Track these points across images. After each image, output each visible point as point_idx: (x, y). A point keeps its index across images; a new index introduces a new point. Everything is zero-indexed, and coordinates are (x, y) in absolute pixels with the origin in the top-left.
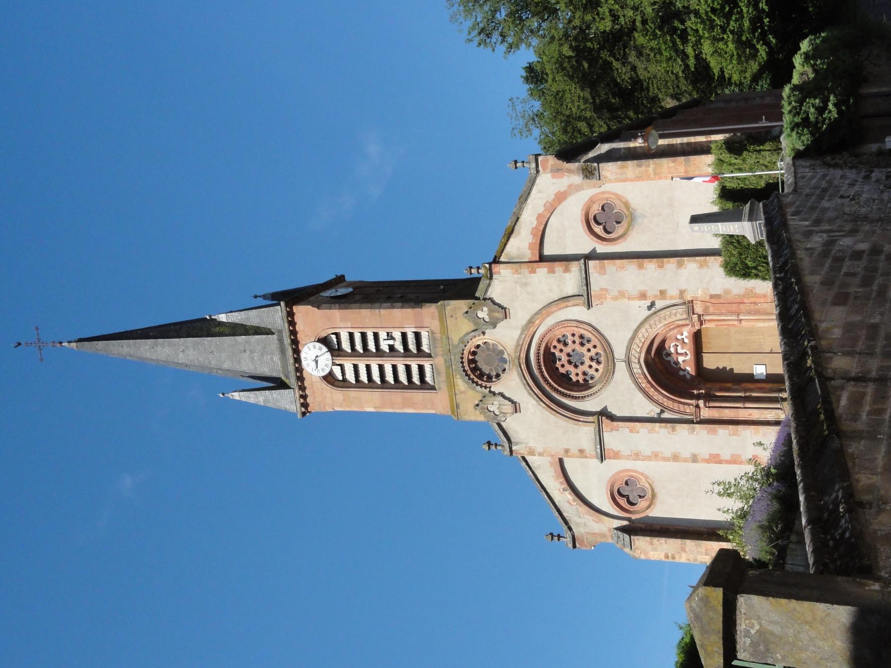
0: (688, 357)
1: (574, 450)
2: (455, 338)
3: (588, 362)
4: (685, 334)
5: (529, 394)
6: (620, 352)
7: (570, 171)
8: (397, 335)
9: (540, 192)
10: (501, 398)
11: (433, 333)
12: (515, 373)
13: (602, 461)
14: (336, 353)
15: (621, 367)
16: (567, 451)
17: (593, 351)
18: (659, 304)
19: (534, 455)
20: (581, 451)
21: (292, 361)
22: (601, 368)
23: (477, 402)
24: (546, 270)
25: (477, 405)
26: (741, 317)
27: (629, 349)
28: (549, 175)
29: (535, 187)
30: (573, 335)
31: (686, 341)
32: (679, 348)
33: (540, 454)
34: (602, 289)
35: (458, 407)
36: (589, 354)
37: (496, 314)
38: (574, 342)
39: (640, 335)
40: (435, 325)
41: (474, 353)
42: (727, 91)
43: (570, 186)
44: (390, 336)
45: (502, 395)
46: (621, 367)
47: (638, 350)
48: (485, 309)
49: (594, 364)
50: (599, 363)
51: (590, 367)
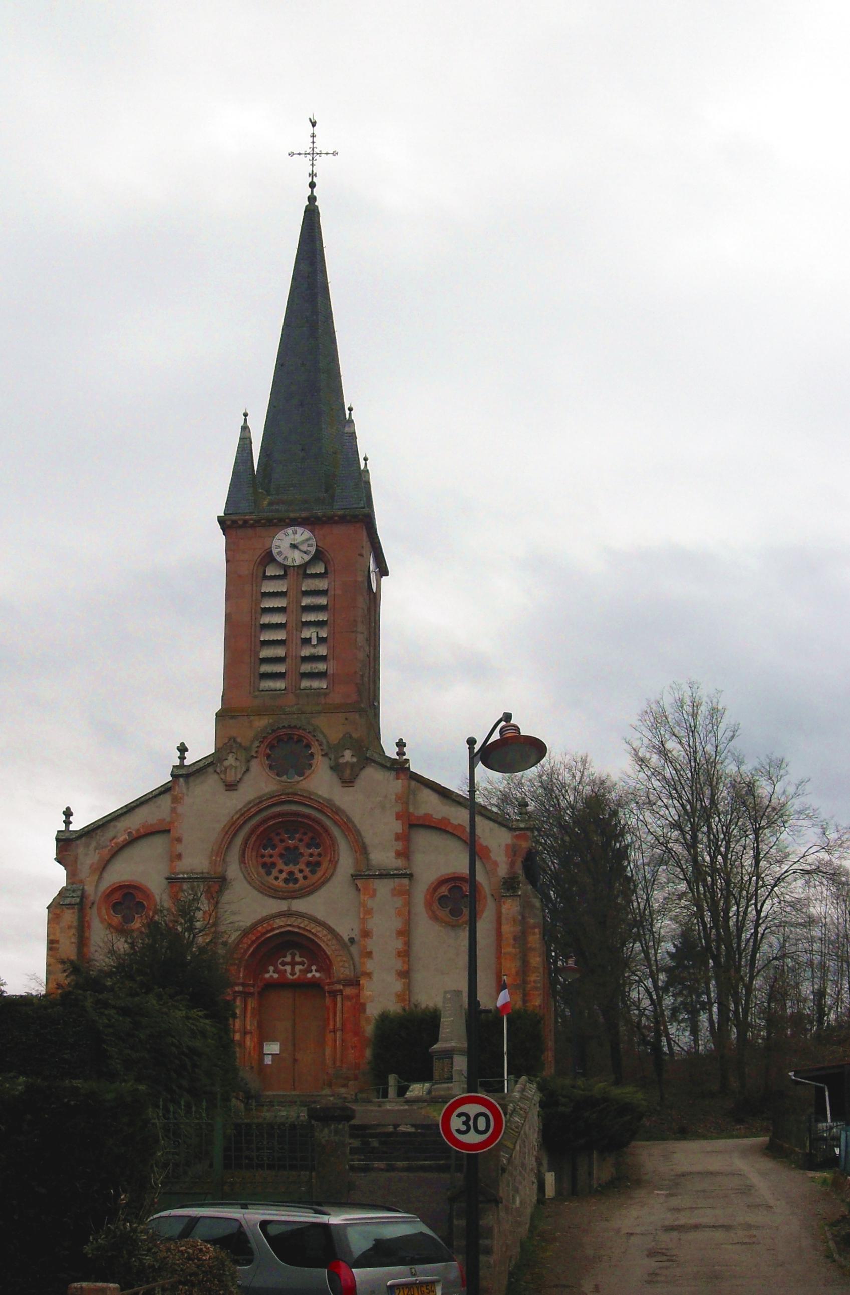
0: (290, 977)
1: (180, 848)
2: (321, 722)
3: (286, 869)
4: (317, 975)
5: (250, 802)
6: (299, 905)
7: (512, 864)
8: (322, 651)
9: (491, 830)
10: (244, 769)
11: (326, 695)
12: (275, 788)
13: (167, 879)
14: (301, 572)
15: (283, 906)
16: (179, 840)
17: (299, 876)
18: (354, 950)
19: (173, 803)
20: (179, 857)
21: (292, 515)
22: (280, 883)
23: (239, 740)
24: (400, 831)
25: (235, 741)
26: (338, 1034)
27: (301, 916)
28: (509, 841)
29: (496, 825)
30: (319, 855)
31: (309, 975)
32: (301, 967)
33: (174, 810)
34: (374, 891)
35: (233, 717)
36: (296, 872)
37: (348, 772)
38: (311, 855)
39: (319, 929)
40: (336, 698)
41: (299, 740)
42: (595, 1007)
43: (496, 864)
44: (321, 641)
45: (248, 770)
46: (283, 906)
47: (302, 926)
48: (354, 760)
49: (284, 876)
50: (286, 881)
51: (281, 872)
